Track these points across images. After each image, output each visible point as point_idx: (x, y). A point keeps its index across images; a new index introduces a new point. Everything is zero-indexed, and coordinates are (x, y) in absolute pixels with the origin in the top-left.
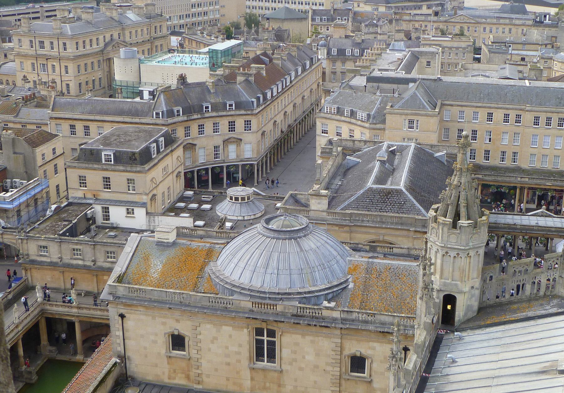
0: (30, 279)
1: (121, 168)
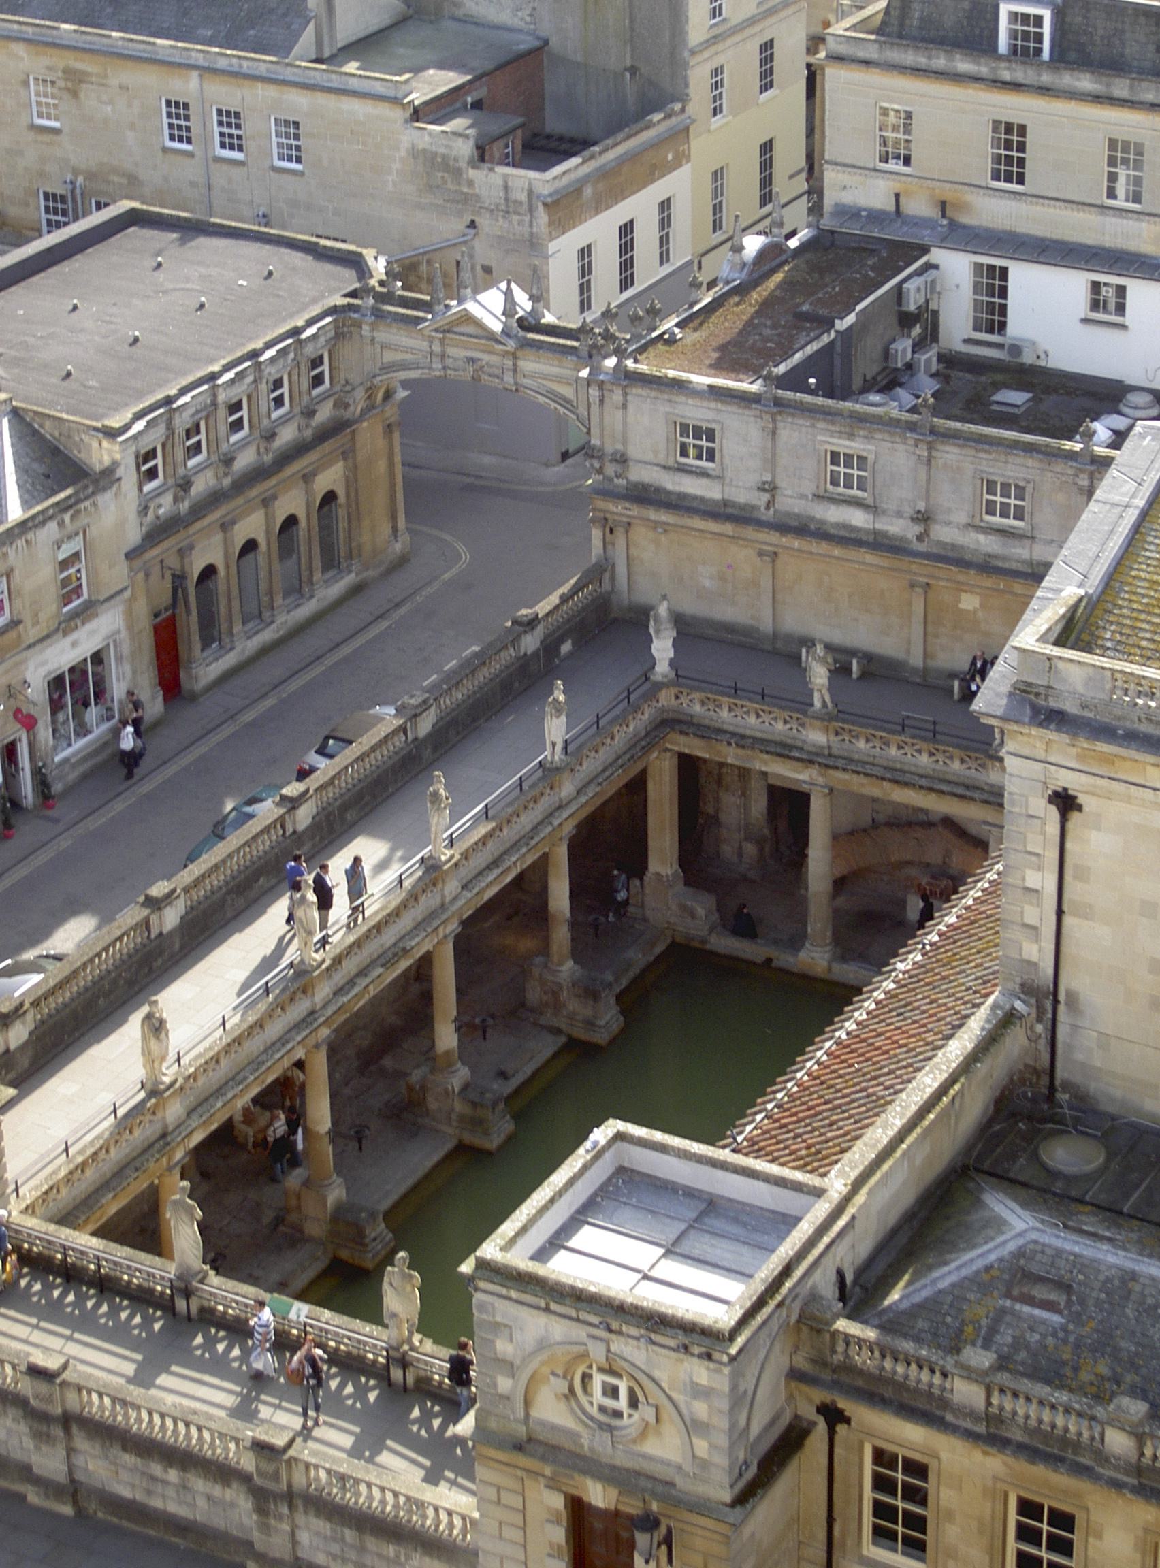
0: (621, 569)
1: (1085, 82)
